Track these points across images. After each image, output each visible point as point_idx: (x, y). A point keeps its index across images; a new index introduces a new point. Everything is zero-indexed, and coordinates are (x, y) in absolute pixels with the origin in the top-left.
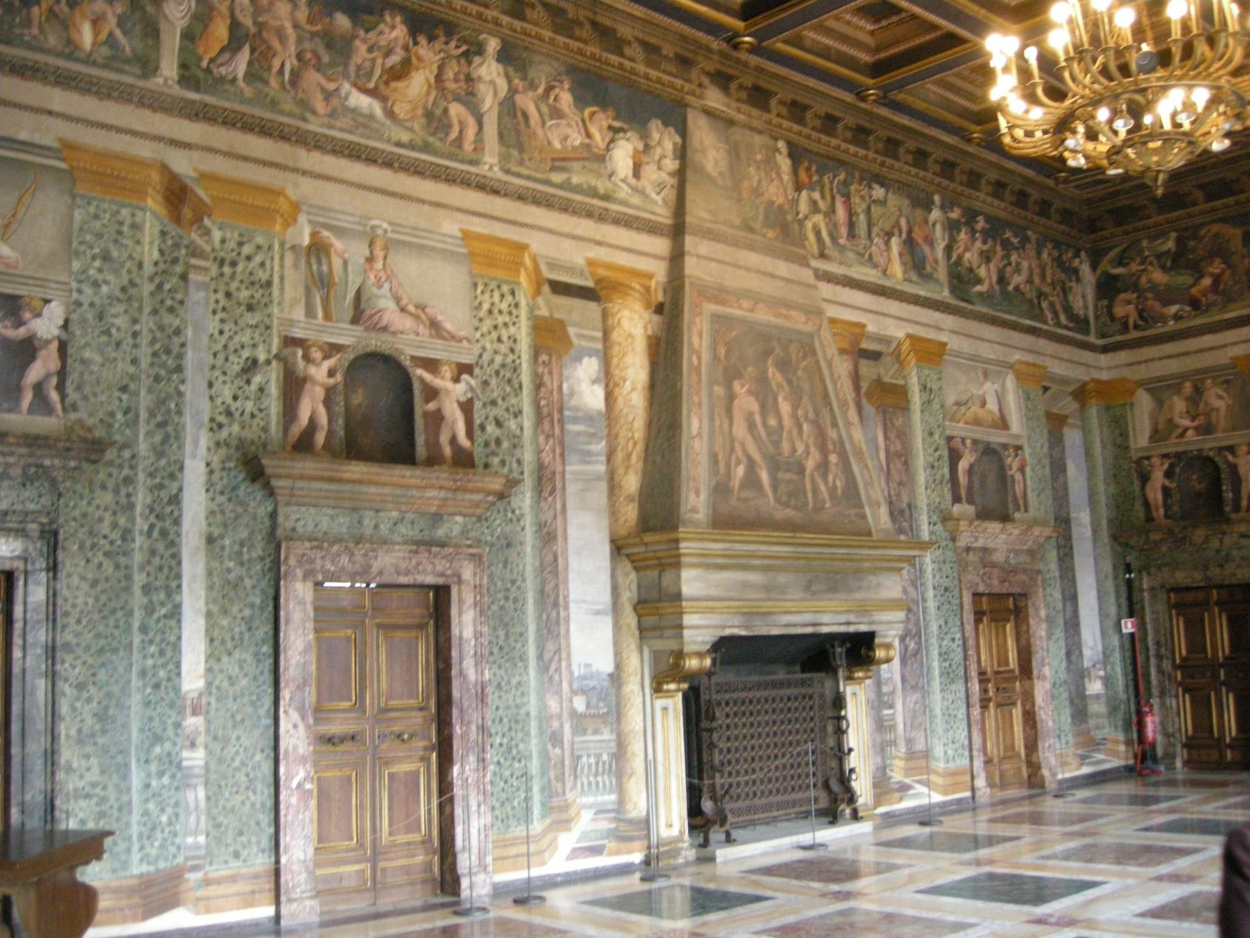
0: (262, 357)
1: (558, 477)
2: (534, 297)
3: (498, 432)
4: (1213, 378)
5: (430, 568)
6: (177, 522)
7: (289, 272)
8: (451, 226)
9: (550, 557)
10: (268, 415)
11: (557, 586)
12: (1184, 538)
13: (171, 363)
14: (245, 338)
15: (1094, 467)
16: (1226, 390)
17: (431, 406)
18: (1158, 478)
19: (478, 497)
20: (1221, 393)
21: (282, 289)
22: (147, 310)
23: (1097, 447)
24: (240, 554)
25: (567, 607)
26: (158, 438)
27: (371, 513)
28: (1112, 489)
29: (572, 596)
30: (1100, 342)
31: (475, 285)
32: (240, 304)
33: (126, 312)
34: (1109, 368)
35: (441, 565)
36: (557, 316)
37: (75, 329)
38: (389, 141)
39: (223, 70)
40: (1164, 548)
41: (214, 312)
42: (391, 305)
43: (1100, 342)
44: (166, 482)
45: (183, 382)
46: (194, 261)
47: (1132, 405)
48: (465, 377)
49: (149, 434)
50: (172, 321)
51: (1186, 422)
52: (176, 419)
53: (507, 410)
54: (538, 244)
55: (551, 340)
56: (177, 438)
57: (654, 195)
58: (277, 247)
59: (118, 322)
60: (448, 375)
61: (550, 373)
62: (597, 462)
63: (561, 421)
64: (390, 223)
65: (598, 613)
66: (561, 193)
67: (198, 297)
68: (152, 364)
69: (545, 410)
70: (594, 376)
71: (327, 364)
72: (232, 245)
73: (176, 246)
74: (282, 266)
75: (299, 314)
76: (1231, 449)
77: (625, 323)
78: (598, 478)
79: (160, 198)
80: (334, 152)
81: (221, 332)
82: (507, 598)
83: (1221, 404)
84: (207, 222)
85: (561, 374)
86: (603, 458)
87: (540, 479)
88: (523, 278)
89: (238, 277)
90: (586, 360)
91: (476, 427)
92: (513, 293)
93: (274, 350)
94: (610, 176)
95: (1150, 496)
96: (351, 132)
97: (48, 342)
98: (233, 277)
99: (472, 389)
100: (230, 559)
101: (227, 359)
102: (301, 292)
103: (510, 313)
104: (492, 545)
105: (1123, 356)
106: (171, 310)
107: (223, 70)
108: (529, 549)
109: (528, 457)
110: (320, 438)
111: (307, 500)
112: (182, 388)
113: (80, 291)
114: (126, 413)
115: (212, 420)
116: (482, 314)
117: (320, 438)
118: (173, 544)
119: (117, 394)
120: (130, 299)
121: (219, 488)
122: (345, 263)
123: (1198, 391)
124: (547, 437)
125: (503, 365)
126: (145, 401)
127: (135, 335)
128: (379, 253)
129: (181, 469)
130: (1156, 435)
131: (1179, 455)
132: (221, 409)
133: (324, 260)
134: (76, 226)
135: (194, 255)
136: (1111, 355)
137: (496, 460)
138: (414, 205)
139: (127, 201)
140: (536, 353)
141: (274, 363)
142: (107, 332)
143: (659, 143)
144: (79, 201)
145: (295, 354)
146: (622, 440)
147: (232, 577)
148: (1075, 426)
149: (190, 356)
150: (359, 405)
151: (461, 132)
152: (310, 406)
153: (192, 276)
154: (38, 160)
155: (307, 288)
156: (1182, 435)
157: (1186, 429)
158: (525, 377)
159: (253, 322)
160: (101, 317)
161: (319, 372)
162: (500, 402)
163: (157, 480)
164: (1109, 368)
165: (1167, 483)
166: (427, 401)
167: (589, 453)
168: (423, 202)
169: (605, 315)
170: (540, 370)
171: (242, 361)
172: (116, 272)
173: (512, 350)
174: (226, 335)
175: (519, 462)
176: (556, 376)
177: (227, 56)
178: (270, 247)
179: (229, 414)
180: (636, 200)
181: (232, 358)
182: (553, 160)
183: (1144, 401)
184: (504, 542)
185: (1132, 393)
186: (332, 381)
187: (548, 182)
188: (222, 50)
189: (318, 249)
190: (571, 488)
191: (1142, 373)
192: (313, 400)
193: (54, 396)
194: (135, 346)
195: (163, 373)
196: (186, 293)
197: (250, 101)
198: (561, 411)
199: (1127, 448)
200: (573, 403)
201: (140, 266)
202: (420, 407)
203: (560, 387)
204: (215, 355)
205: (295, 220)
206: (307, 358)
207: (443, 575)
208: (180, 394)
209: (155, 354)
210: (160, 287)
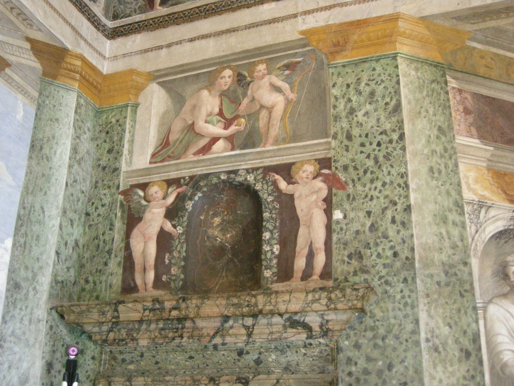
4: (269, 62)
12: (180, 320)
15: (47, 177)
16: (287, 79)
18: (155, 219)
20: (280, 83)
23: (62, 152)
28: (77, 232)
30: (110, 24)
34: (115, 58)
40: (143, 342)
43: (110, 24)
47: (136, 106)
51: (217, 130)
76: (286, 171)
83: (278, 101)
95: (137, 245)
105: (138, 41)
123: (242, 81)
130: (165, 151)
131: (195, 182)
136: (120, 40)
148: (24, 93)
156: (206, 149)
157: (215, 140)
164: (115, 58)
165: (168, 226)
183: (155, 101)
185: (139, 89)
191: (164, 60)
199: (116, 170)
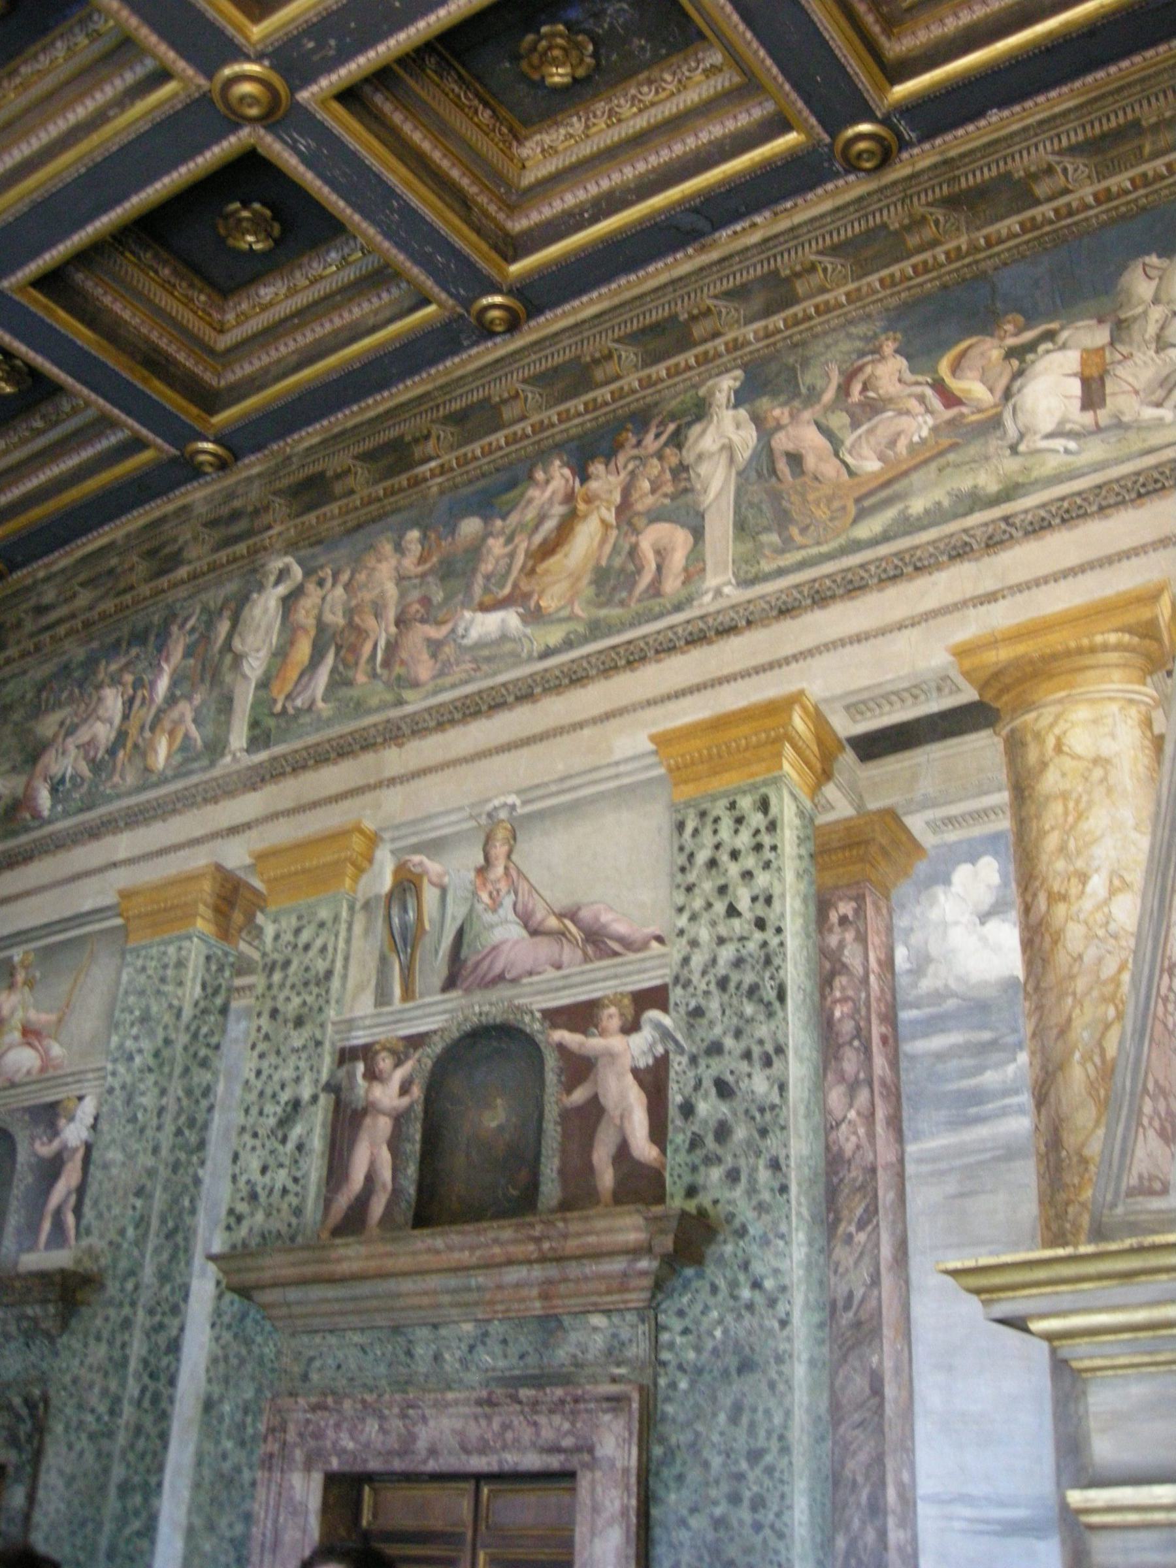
0: (306, 1093)
1: (883, 1178)
2: (816, 790)
3: (724, 1109)
5: (527, 1434)
6: (172, 1382)
7: (356, 944)
8: (632, 741)
9: (860, 1383)
10: (304, 1187)
11: (878, 1460)
13: (192, 1137)
14: (287, 1073)
17: (579, 1096)
19: (617, 1265)
21: (344, 977)
22: (178, 1070)
24: (242, 1426)
25: (908, 1519)
26: (165, 1256)
27: (423, 1333)
29: (926, 1486)
31: (681, 826)
32: (285, 1022)
33: (156, 1083)
35: (552, 1427)
36: (873, 805)
37: (104, 1126)
38: (530, 659)
39: (299, 702)
41: (253, 1047)
42: (516, 931)
44: (166, 1321)
45: (202, 1163)
46: (238, 982)
48: (654, 1014)
49: (157, 1250)
50: (201, 1077)
52: (188, 1219)
53: (747, 1055)
54: (821, 682)
55: (861, 864)
56: (186, 1250)
57: (1149, 413)
58: (344, 914)
59: (144, 1100)
60: (615, 1023)
61: (862, 939)
62: (1004, 1112)
63: (892, 1042)
64: (518, 793)
65: (1012, 1529)
66: (883, 550)
67: (238, 1028)
68: (173, 1149)
69: (847, 1027)
70: (987, 900)
71: (399, 1075)
72: (288, 937)
73: (221, 969)
74: (348, 941)
75: (365, 1006)
77: (1080, 741)
78: (1009, 1153)
79: (209, 913)
80: (440, 726)
81: (259, 1073)
82: (735, 1499)
84: (260, 919)
85: (890, 929)
86: (1025, 1098)
87: (832, 1194)
88: (790, 766)
89: (288, 983)
90: (962, 874)
91: (673, 1112)
92: (764, 805)
93: (324, 1076)
94: (1014, 449)
96: (465, 682)
97: (76, 1150)
98: (282, 986)
99: (666, 1035)
100: (229, 1437)
101: (261, 1113)
102: (372, 964)
103: (758, 847)
104: (699, 1371)
106: (204, 1063)
107: (299, 702)
108: (800, 1372)
109: (799, 1147)
110: (377, 1207)
111: (317, 1322)
112: (201, 1172)
113: (114, 1074)
114: (137, 1227)
115: (231, 1212)
116: (691, 877)
117: (377, 1207)
118: (164, 1416)
119: (132, 1200)
120: (161, 1065)
121: (226, 1319)
122: (444, 890)
124: (853, 1089)
125: (738, 963)
126: (159, 1200)
127: (161, 1111)
128: (499, 850)
129: (186, 1298)
132: (244, 1193)
133: (411, 903)
134: (122, 990)
135: (240, 972)
137: (716, 1174)
138: (565, 740)
139: (166, 936)
140: (822, 906)
141: (323, 1099)
142: (133, 1119)
143: (1156, 301)
144: (129, 958)
145: (351, 1076)
146: (1081, 1034)
147: (226, 1466)
149: (217, 1119)
150: (501, 1128)
151: (659, 568)
152: (371, 1154)
153: (235, 1005)
154: (97, 927)
155: (383, 960)
158: (795, 971)
159: (297, 1043)
160: (129, 1101)
161: (387, 1095)
162: (729, 1042)
163: (158, 1318)
166: (569, 1089)
167: (977, 1097)
168: (580, 725)
169: (1015, 746)
170: (833, 941)
171: (279, 1110)
172: (152, 1034)
173: (760, 924)
174: (264, 1077)
175: (775, 1165)
176: (874, 940)
177: (305, 679)
178: (336, 919)
179: (253, 1196)
180: (1095, 451)
181: (270, 1108)
182: (858, 500)
184: (732, 1362)
186: (405, 1101)
187: (857, 546)
188: (301, 675)
189: (407, 884)
190: (919, 1198)
192: (373, 1144)
193: (70, 1219)
194: (159, 1128)
195: (183, 1156)
196: (224, 1031)
197: (329, 722)
198: (890, 1018)
200: (926, 984)
201: (178, 1015)
202: (556, 1100)
203: (888, 963)
204: (247, 1111)
205: (371, 860)
206: (372, 1075)
207: (555, 1449)
208: (197, 1181)
209: (179, 1132)
210: (195, 1036)
